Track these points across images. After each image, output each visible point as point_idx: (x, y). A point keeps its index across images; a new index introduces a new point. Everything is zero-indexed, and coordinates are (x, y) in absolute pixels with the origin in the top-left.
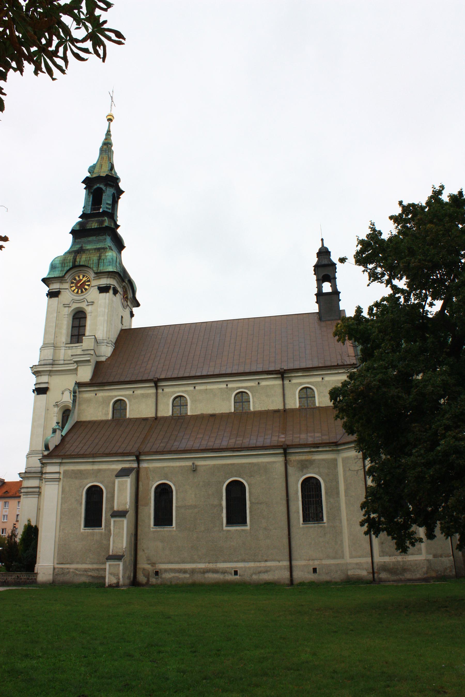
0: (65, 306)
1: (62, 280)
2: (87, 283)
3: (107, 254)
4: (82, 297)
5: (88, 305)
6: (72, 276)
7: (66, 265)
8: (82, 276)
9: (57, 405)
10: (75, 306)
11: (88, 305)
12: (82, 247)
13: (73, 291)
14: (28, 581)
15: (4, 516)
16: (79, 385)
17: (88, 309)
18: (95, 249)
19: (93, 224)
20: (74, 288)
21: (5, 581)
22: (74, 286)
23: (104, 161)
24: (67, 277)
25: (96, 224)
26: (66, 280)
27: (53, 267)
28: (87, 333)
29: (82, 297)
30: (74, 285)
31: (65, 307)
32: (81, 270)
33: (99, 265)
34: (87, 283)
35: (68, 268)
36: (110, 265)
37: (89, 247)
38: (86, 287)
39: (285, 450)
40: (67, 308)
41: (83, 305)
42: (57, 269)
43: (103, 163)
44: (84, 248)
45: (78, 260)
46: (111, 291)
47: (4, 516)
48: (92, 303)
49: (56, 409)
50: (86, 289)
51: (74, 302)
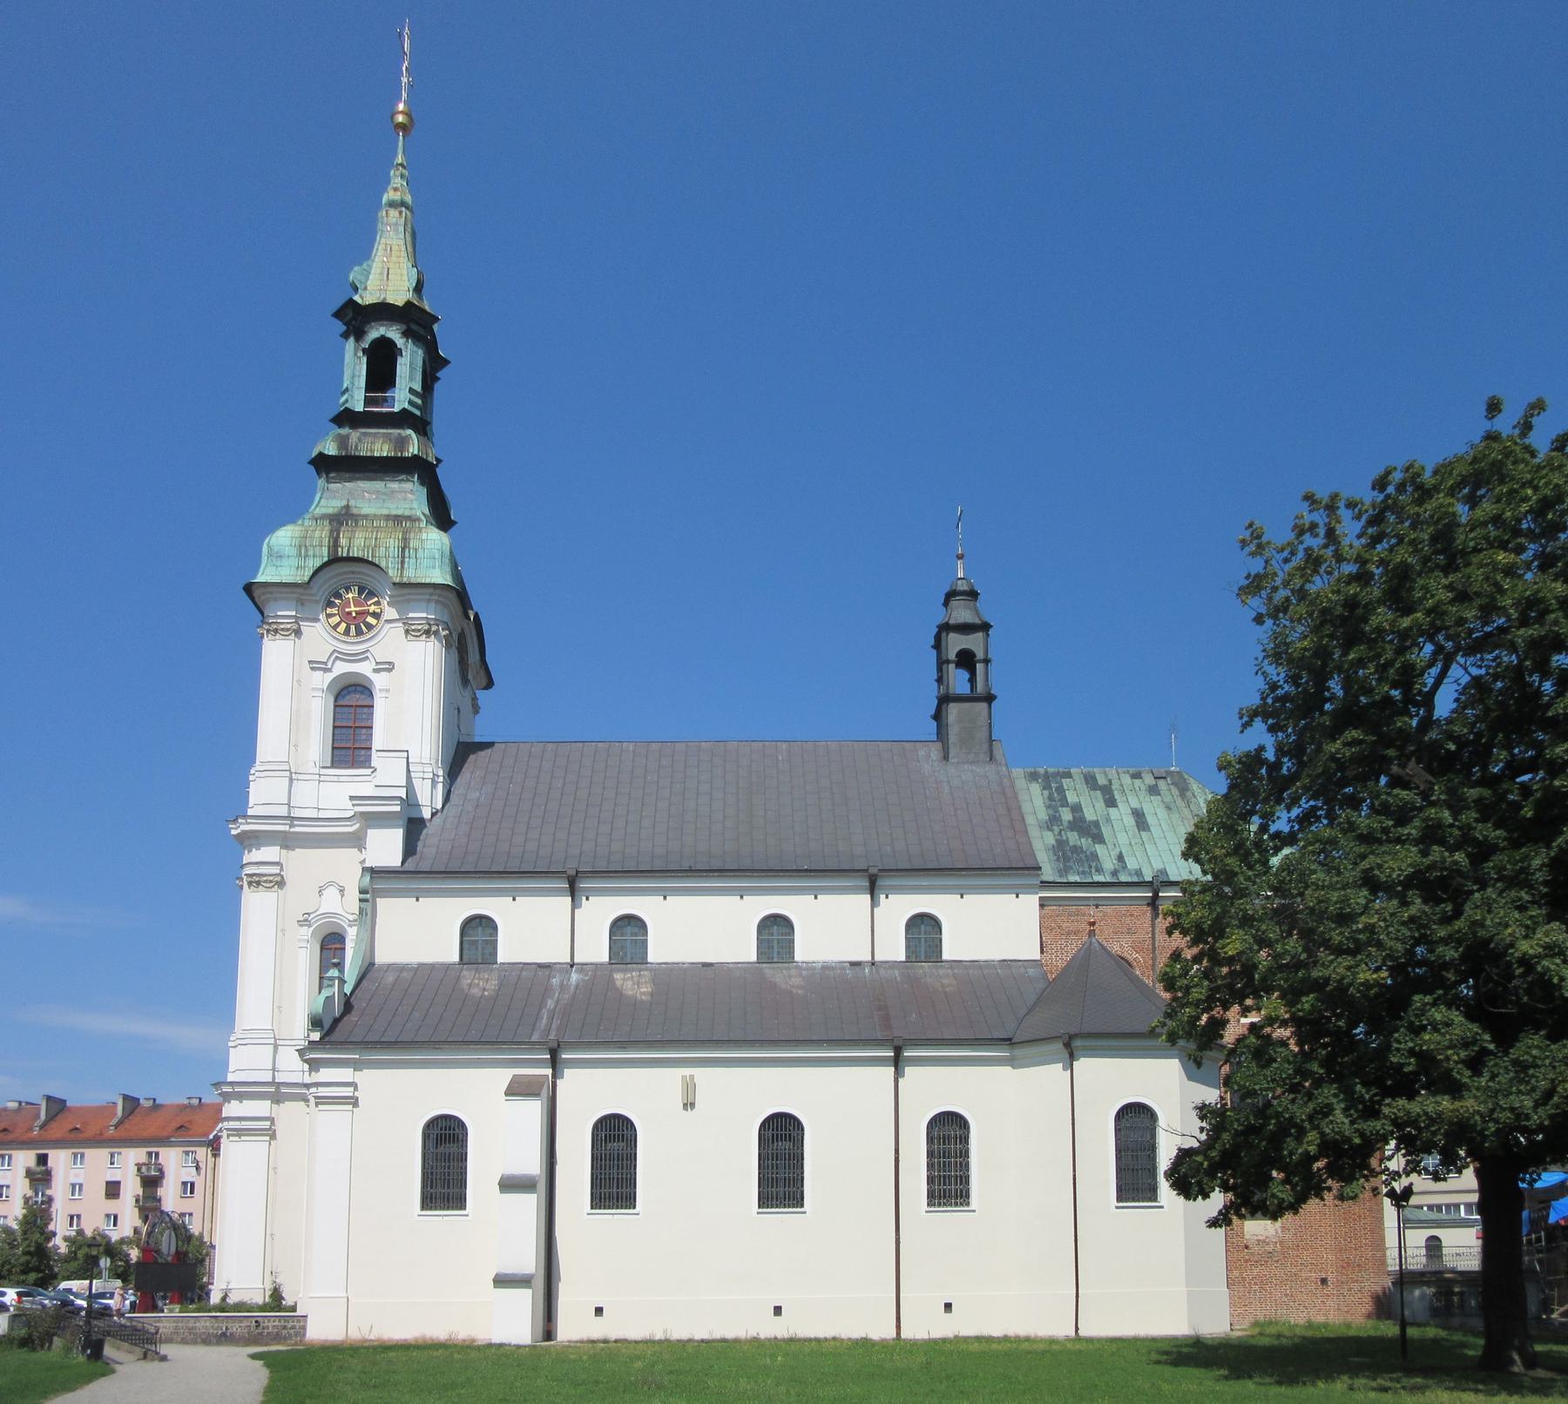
0: (315, 665)
3: (424, 536)
7: (311, 553)
8: (356, 588)
9: (306, 920)
10: (341, 668)
12: (347, 507)
13: (335, 627)
14: (285, 1332)
15: (73, 1186)
16: (375, 873)
17: (379, 681)
18: (388, 517)
19: (377, 446)
21: (224, 1334)
22: (335, 615)
23: (394, 259)
25: (386, 447)
28: (377, 743)
30: (334, 611)
32: (353, 573)
33: (403, 563)
35: (318, 563)
36: (434, 567)
37: (366, 509)
39: (898, 1050)
41: (365, 668)
42: (285, 562)
43: (391, 266)
44: (355, 511)
45: (343, 541)
47: (73, 1186)
48: (389, 667)
49: (306, 932)
50: (370, 627)
51: (337, 657)
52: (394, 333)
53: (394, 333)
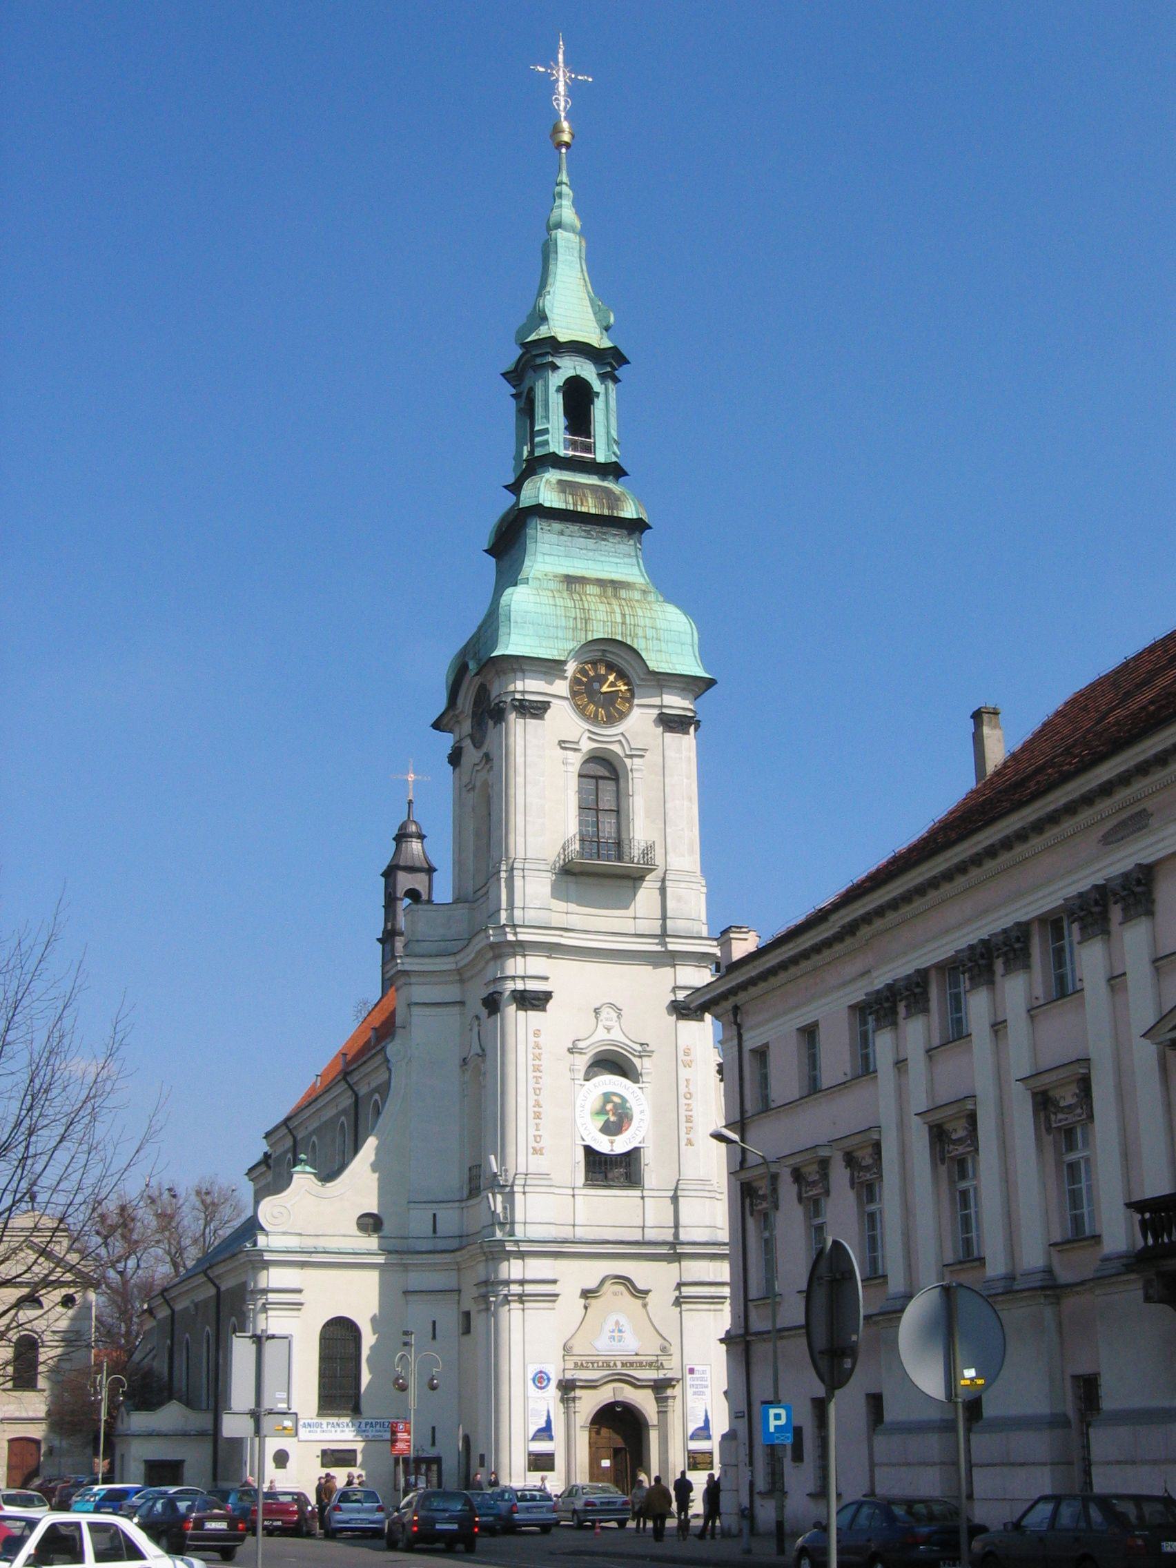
24: (460, 701)
52: (588, 371)
53: (588, 371)
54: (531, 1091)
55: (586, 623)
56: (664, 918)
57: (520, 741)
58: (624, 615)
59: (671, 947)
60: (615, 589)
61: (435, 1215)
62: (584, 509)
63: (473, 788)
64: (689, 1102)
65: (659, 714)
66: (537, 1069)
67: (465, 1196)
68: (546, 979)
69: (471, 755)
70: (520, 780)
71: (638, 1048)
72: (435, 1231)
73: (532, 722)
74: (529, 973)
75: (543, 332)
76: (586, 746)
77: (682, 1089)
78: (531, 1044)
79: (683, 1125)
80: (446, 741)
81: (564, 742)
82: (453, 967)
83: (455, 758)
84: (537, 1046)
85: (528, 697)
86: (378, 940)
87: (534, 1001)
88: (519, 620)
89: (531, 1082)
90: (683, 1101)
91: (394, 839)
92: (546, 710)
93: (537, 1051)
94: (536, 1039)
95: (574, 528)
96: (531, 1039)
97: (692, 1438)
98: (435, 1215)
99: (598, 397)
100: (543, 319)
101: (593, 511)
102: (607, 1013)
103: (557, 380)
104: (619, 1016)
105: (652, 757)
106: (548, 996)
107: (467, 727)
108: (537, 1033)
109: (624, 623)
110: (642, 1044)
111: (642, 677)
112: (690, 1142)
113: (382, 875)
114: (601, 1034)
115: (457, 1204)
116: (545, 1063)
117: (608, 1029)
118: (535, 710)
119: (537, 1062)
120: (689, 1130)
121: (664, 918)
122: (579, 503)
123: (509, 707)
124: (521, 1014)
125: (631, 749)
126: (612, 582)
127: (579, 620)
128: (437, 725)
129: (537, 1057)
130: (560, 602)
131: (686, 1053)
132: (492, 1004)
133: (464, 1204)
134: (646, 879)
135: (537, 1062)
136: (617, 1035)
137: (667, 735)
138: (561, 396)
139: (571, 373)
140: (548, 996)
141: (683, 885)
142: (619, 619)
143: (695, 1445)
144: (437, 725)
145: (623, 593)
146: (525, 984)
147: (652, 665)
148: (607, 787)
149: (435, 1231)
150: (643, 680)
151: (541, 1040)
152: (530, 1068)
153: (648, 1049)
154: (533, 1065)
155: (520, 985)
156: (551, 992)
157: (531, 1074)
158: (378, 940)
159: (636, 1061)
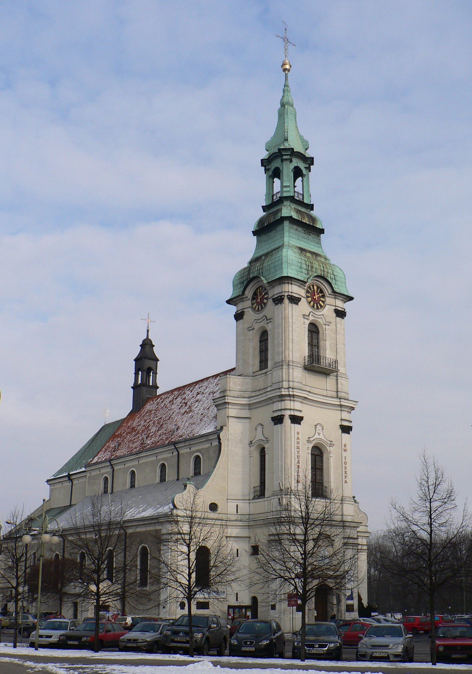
0: (251, 329)
1: (243, 298)
2: (265, 297)
4: (262, 315)
5: (268, 323)
6: (252, 289)
11: (268, 323)
20: (255, 304)
22: (255, 303)
24: (246, 292)
26: (247, 297)
27: (234, 286)
29: (262, 315)
31: (249, 330)
34: (265, 297)
38: (265, 301)
40: (251, 331)
46: (286, 301)
54: (296, 457)
55: (312, 268)
56: (337, 392)
57: (290, 313)
58: (323, 267)
59: (342, 403)
60: (316, 256)
61: (237, 505)
62: (305, 221)
63: (253, 329)
64: (346, 466)
65: (335, 310)
66: (298, 448)
67: (251, 498)
68: (301, 411)
69: (250, 315)
70: (290, 329)
71: (329, 442)
72: (237, 512)
73: (294, 305)
74: (295, 408)
75: (286, 145)
76: (311, 318)
77: (344, 461)
78: (296, 438)
79: (344, 475)
80: (233, 309)
81: (305, 315)
82: (248, 403)
83: (239, 316)
84: (298, 438)
85: (293, 295)
86: (132, 387)
87: (296, 420)
88: (290, 263)
89: (296, 453)
90: (344, 465)
91: (141, 346)
92: (299, 301)
93: (298, 440)
94: (298, 436)
95: (300, 229)
96: (296, 436)
97: (347, 599)
98: (237, 505)
99: (305, 176)
100: (286, 140)
101: (307, 222)
102: (318, 426)
103: (292, 166)
104: (323, 429)
105: (332, 326)
106: (301, 418)
107: (248, 303)
108: (298, 433)
109: (324, 271)
110: (330, 441)
111: (330, 293)
112: (346, 482)
113: (135, 360)
114: (317, 436)
115: (248, 501)
116: (300, 445)
117: (319, 434)
118: (295, 300)
119: (298, 445)
120: (346, 477)
121: (337, 392)
122: (303, 219)
123: (286, 297)
124: (292, 425)
125: (326, 322)
126: (314, 253)
127: (310, 267)
128: (229, 302)
129: (298, 443)
130: (303, 258)
131: (345, 446)
132: (278, 420)
133: (251, 501)
134: (331, 375)
135: (298, 445)
136: (321, 436)
137: (337, 318)
138: (293, 173)
139: (296, 165)
140: (301, 418)
141: (343, 379)
142: (322, 269)
143: (350, 602)
144: (229, 302)
145: (319, 258)
146: (294, 413)
147: (336, 290)
148: (315, 335)
149: (237, 512)
150: (330, 294)
151: (300, 436)
152: (296, 448)
153: (332, 443)
154: (297, 446)
155: (292, 413)
156: (303, 417)
157: (296, 450)
158: (132, 387)
159: (328, 448)
